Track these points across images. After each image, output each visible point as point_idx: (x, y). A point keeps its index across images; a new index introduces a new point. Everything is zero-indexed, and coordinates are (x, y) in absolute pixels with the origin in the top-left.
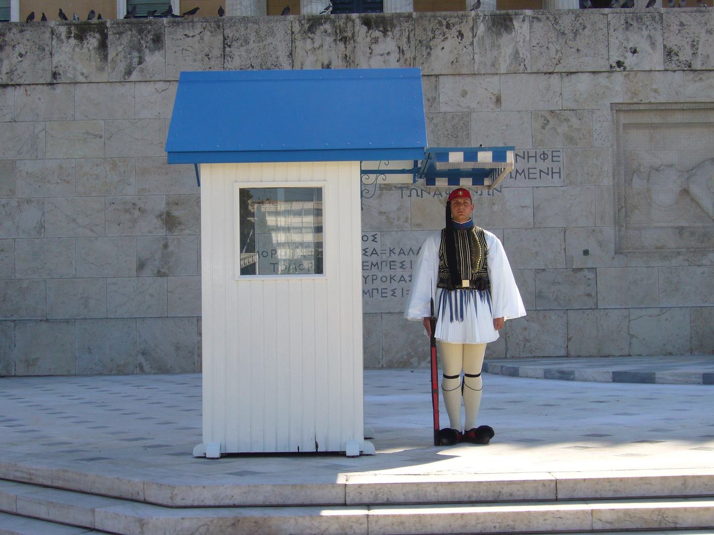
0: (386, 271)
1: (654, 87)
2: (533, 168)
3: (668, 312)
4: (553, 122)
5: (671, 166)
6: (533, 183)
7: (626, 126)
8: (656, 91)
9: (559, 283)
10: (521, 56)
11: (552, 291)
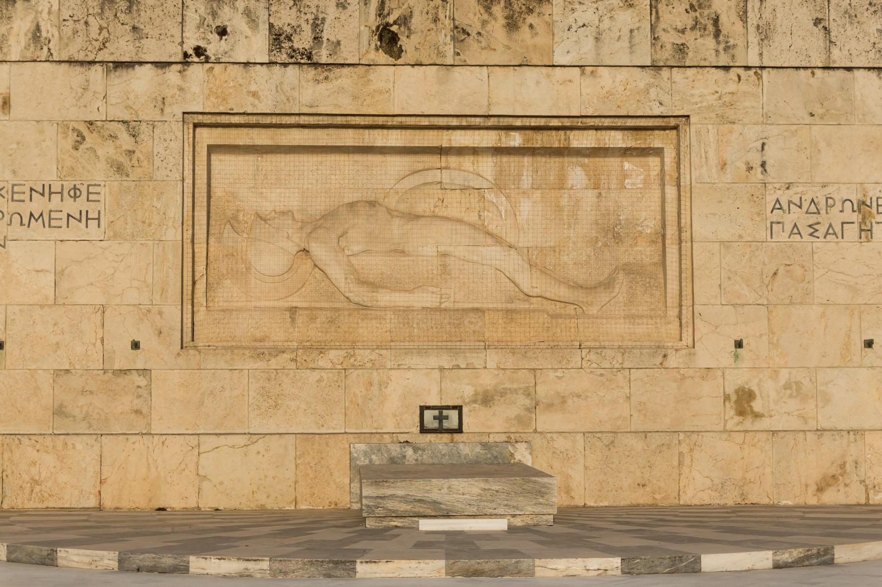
1: (253, 88)
2: (57, 211)
3: (260, 441)
4: (91, 139)
5: (283, 213)
6: (55, 234)
7: (212, 149)
8: (255, 94)
9: (91, 392)
10: (44, 34)
11: (80, 404)
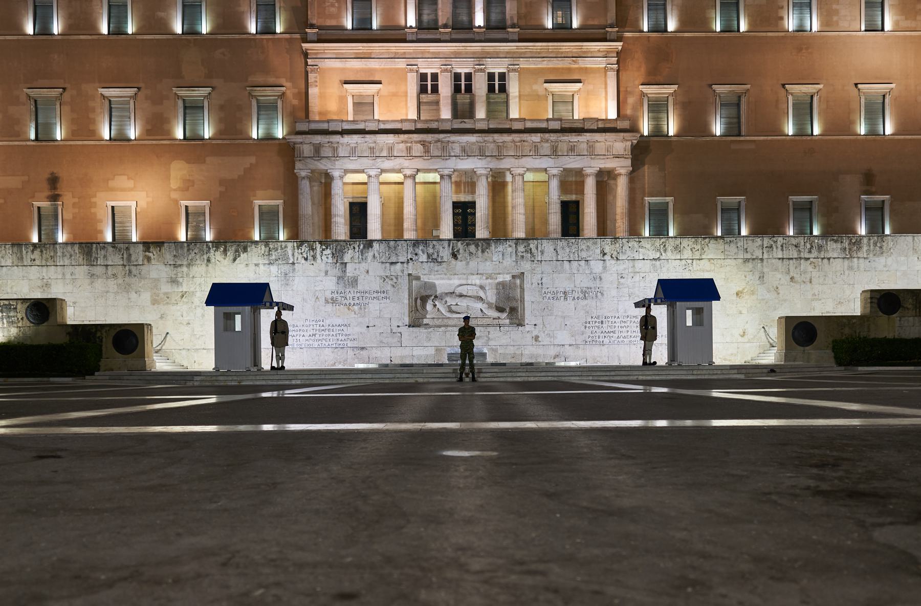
0: (327, 332)
4: (387, 280)
